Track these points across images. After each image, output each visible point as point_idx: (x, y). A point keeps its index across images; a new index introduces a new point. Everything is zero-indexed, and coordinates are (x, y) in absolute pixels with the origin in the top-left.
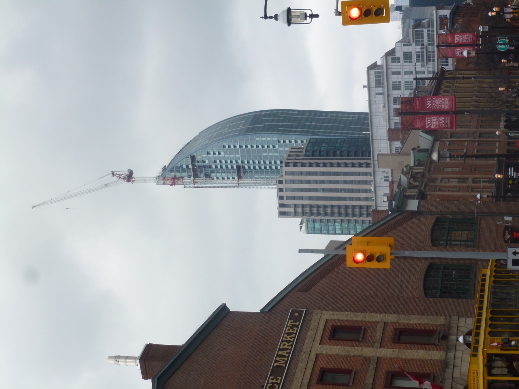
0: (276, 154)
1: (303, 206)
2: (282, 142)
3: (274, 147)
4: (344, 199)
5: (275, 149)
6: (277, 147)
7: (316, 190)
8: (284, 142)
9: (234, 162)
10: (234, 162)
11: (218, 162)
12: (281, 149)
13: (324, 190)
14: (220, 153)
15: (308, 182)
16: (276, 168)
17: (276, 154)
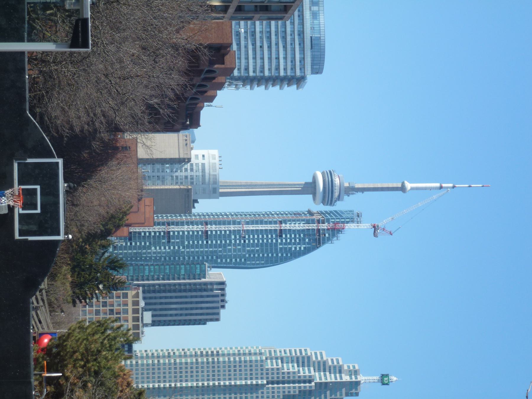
0: (248, 249)
1: (205, 290)
2: (243, 260)
3: (250, 255)
4: (176, 297)
5: (249, 254)
6: (247, 256)
7: (197, 303)
8: (241, 260)
9: (284, 241)
10: (284, 241)
11: (298, 240)
12: (244, 253)
13: (191, 303)
14: (296, 248)
15: (201, 308)
16: (249, 236)
17: (248, 249)
